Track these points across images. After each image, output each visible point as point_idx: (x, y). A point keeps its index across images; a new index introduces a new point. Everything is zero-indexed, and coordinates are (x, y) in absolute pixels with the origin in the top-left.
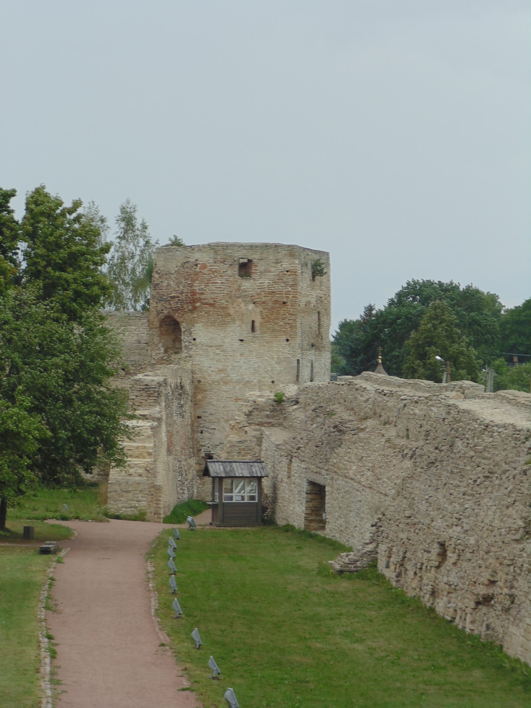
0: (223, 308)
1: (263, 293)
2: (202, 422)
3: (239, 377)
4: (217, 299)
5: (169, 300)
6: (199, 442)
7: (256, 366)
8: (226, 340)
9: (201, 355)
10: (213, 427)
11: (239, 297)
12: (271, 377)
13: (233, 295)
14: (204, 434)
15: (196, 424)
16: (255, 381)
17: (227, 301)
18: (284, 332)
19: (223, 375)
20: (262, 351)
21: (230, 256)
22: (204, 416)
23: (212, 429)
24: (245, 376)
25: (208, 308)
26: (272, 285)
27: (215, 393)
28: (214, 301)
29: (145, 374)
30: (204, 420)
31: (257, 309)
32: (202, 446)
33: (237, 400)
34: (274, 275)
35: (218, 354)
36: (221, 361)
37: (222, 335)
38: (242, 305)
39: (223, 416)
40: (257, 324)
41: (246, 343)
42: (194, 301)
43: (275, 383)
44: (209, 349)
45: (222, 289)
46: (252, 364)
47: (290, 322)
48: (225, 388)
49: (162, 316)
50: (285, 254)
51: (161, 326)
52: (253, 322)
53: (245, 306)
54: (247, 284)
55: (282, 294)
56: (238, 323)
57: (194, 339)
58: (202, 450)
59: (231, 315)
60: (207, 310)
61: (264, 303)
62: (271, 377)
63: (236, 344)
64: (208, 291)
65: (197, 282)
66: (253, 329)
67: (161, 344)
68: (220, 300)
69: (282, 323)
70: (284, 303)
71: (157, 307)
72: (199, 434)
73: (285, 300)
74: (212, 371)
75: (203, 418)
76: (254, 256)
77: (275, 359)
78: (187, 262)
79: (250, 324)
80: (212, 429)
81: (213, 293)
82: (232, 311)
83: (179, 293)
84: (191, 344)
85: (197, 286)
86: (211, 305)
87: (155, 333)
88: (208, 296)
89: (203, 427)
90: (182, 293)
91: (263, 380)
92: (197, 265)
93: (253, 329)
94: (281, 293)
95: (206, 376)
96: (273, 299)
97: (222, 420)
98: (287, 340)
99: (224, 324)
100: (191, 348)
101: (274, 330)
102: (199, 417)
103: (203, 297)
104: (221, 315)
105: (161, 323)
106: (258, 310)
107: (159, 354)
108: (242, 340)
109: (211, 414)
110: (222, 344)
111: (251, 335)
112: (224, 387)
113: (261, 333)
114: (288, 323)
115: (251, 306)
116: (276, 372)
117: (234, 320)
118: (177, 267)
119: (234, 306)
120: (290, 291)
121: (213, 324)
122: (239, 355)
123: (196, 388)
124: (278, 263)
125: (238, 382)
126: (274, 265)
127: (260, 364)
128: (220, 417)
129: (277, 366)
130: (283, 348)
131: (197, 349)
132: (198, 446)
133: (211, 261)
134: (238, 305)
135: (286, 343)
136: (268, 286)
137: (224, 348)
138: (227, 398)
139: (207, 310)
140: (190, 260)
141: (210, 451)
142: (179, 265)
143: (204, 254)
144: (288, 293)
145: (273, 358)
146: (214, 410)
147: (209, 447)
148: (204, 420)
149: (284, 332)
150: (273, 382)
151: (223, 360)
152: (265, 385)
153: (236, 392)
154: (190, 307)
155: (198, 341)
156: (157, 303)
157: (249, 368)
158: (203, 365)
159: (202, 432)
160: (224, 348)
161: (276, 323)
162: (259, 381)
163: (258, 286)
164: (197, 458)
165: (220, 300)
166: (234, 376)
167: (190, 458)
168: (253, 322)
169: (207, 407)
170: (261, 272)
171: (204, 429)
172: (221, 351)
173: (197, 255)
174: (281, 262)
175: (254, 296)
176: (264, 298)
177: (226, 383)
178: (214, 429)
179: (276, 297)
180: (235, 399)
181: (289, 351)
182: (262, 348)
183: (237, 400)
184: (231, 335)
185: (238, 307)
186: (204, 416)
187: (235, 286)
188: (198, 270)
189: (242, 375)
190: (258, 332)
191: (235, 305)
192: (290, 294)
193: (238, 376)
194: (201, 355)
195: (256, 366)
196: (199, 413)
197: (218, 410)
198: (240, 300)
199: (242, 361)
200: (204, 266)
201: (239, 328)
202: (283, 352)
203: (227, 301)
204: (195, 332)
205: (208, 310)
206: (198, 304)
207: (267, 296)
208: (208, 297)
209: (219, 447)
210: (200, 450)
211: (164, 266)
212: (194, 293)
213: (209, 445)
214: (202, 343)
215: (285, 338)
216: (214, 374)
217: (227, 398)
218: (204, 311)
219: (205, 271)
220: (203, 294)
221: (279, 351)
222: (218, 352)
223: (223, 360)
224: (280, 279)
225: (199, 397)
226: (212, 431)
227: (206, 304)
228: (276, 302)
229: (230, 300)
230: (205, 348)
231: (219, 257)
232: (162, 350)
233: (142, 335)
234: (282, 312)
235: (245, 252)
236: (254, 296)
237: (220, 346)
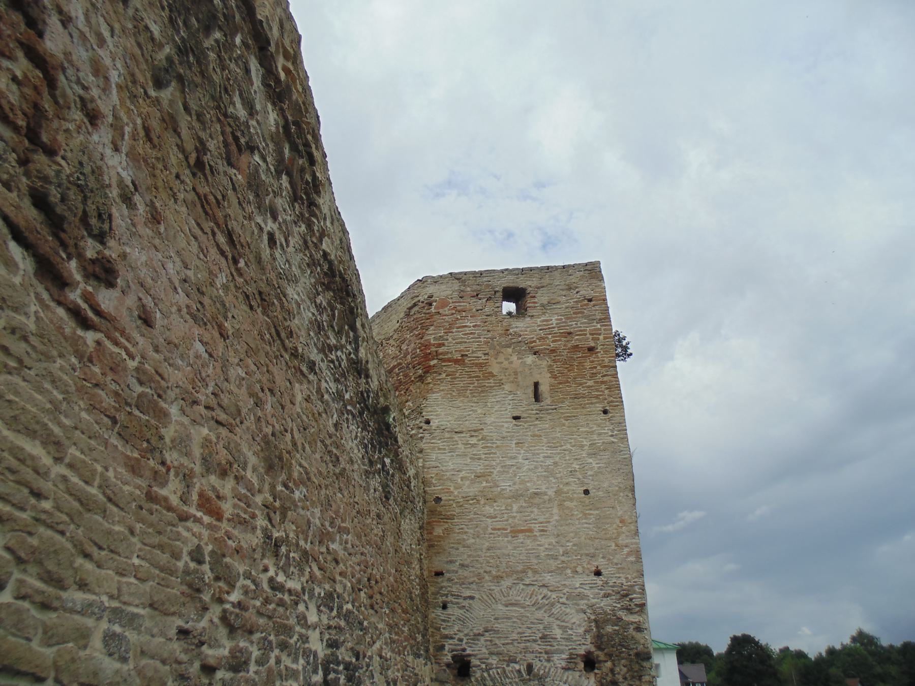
0: (480, 365)
2: (445, 584)
3: (516, 487)
6: (438, 629)
7: (549, 462)
8: (489, 420)
9: (439, 449)
10: (468, 593)
11: (508, 346)
12: (583, 483)
13: (495, 343)
14: (449, 611)
15: (432, 589)
16: (551, 492)
17: (485, 354)
18: (597, 397)
19: (484, 484)
20: (558, 435)
21: (488, 286)
22: (448, 571)
23: (465, 598)
24: (528, 484)
27: (471, 520)
28: (462, 356)
29: (216, 230)
30: (449, 580)
31: (540, 362)
32: (447, 637)
33: (515, 533)
35: (473, 446)
36: (479, 459)
38: (514, 358)
39: (488, 569)
40: (544, 388)
41: (526, 422)
42: (427, 357)
43: (591, 494)
44: (456, 437)
46: (542, 459)
47: (605, 379)
48: (489, 510)
50: (582, 276)
52: (536, 385)
53: (518, 359)
54: (520, 325)
55: (585, 335)
56: (507, 387)
57: (428, 422)
58: (447, 648)
59: (494, 376)
61: (553, 351)
62: (583, 483)
63: (506, 425)
64: (450, 339)
65: (432, 328)
66: (537, 397)
68: (473, 352)
69: (590, 383)
70: (591, 349)
72: (439, 611)
73: (593, 345)
74: (462, 479)
75: (447, 575)
76: (529, 283)
77: (586, 448)
78: (415, 305)
79: (532, 388)
80: (465, 598)
81: (461, 343)
82: (495, 369)
84: (421, 431)
85: (431, 336)
86: (456, 361)
88: (453, 349)
89: (447, 595)
91: (566, 489)
92: (430, 304)
93: (537, 397)
94: (582, 333)
95: (452, 489)
97: (487, 578)
98: (605, 412)
99: (482, 392)
100: (422, 438)
101: (576, 397)
102: (439, 574)
103: (441, 350)
104: (478, 377)
108: (516, 418)
109: (462, 565)
110: (482, 427)
111: (537, 406)
112: (487, 508)
113: (553, 401)
114: (602, 382)
115: (530, 359)
116: (590, 473)
117: (501, 384)
119: (499, 360)
120: (600, 329)
121: (461, 393)
122: (514, 446)
123: (432, 512)
124: (570, 289)
125: (516, 496)
126: (564, 293)
127: (557, 459)
128: (482, 571)
129: (591, 460)
130: (599, 425)
131: (433, 438)
132: (438, 638)
133: (456, 294)
134: (507, 359)
135: (602, 416)
137: (485, 433)
138: (494, 529)
140: (420, 298)
141: (464, 650)
142: (402, 315)
143: (443, 287)
144: (595, 334)
145: (583, 446)
146: (469, 556)
147: (461, 640)
148: (449, 580)
149: (597, 397)
150: (586, 492)
151: (483, 456)
152: (571, 500)
153: (515, 517)
157: (536, 468)
158: (444, 468)
159: (445, 607)
160: (485, 433)
161: (581, 384)
162: (558, 492)
163: (539, 326)
164: (436, 667)
165: (473, 352)
166: (506, 485)
167: (417, 656)
168: (536, 385)
169: (453, 552)
170: (542, 305)
171: (450, 598)
172: (479, 440)
173: (431, 289)
174: (577, 288)
175: (535, 342)
177: (492, 500)
178: (472, 598)
180: (511, 532)
181: (612, 431)
182: (558, 429)
183: (515, 533)
184: (497, 411)
185: (506, 363)
186: (448, 571)
187: (500, 329)
188: (433, 310)
189: (523, 482)
190: (547, 401)
191: (501, 358)
192: (600, 334)
193: (514, 484)
194: (439, 449)
195: (549, 462)
196: (438, 563)
197: (479, 556)
198: (510, 350)
199: (520, 457)
200: (444, 303)
201: (510, 397)
202: (600, 434)
203: (485, 354)
204: (430, 409)
206: (432, 363)
207: (560, 340)
208: (452, 347)
209: (482, 639)
210: (442, 647)
211: (379, 334)
212: (427, 346)
213: (461, 635)
215: (600, 407)
216: (467, 483)
217: (494, 529)
218: (445, 371)
219: (446, 310)
220: (444, 345)
221: (592, 433)
222: (474, 441)
223: (483, 456)
224: (579, 313)
225: (438, 531)
226: (466, 603)
227: (449, 360)
228: (576, 348)
229: (491, 352)
230: (447, 435)
231: (469, 289)
234: (588, 365)
235: (511, 277)
236: (535, 342)
237: (475, 431)
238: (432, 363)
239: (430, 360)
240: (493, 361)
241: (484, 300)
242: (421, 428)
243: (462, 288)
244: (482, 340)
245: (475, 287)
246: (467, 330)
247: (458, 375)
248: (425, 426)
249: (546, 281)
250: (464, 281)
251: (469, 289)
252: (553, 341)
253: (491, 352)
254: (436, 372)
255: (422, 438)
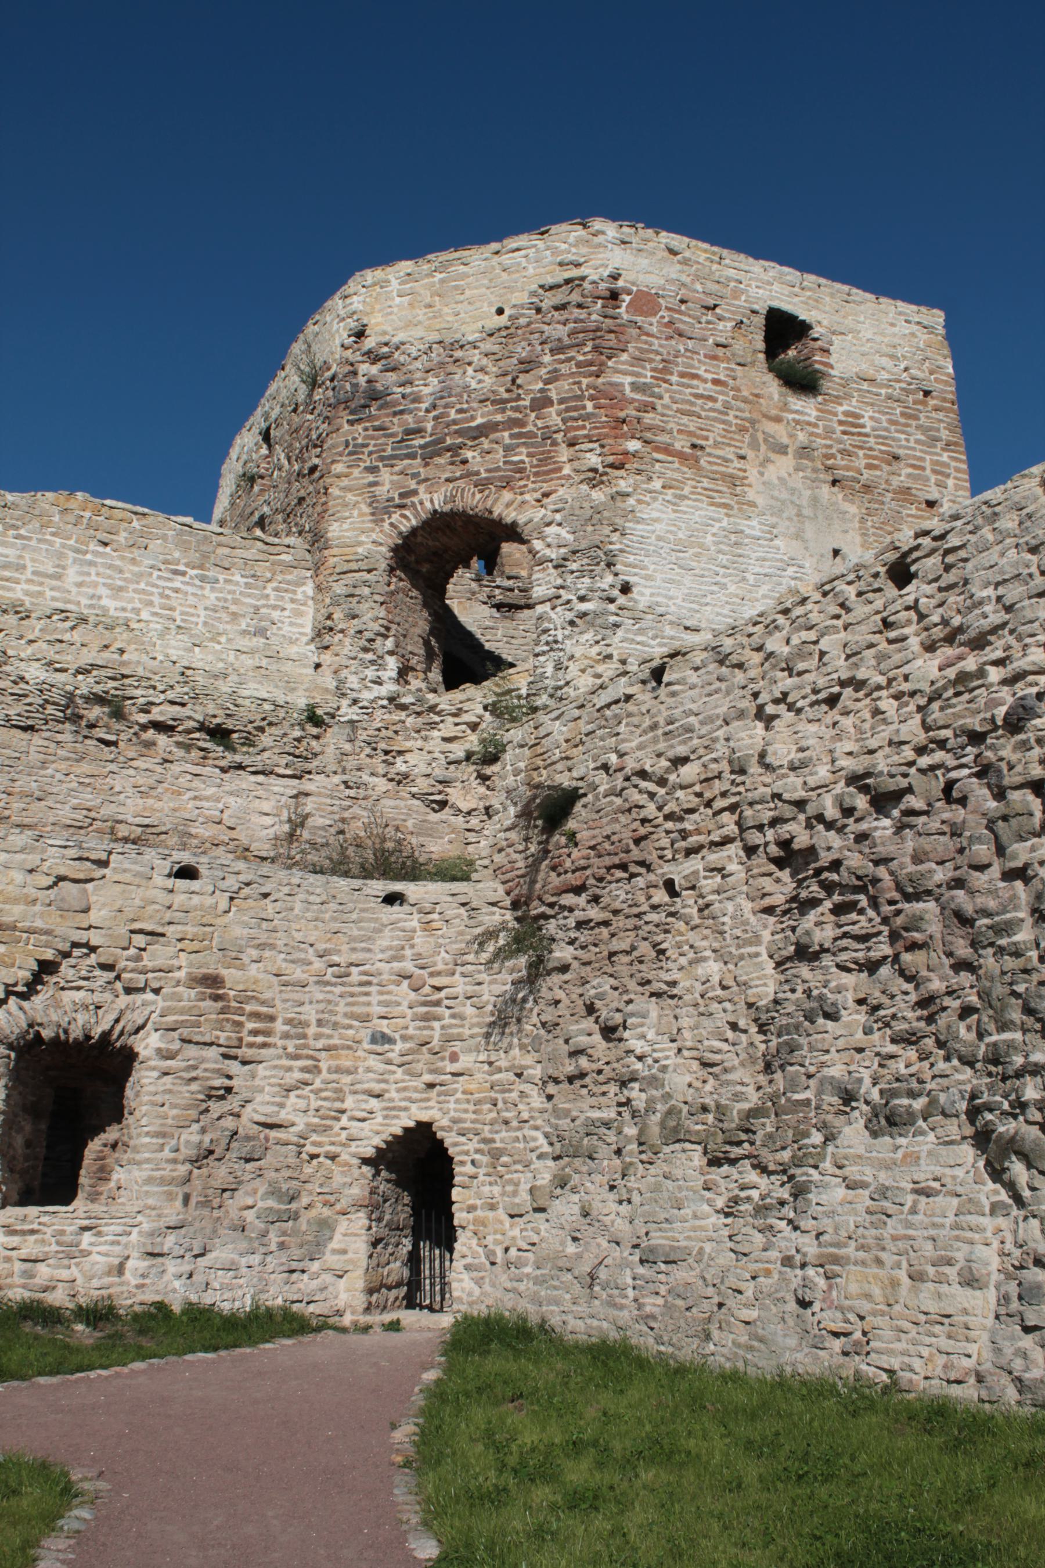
1: (861, 453)
4: (707, 439)
5: (454, 449)
25: (674, 470)
26: (886, 430)
28: (694, 446)
34: (889, 397)
37: (732, 589)
45: (719, 405)
49: (408, 521)
51: (392, 570)
57: (626, 589)
60: (670, 474)
61: (867, 488)
64: (666, 400)
65: (625, 357)
67: (390, 643)
68: (716, 445)
71: (375, 484)
73: (934, 494)
83: (517, 409)
84: (612, 607)
86: (682, 456)
87: (366, 591)
90: (541, 403)
92: (614, 296)
96: (896, 482)
100: (617, 625)
105: (396, 550)
106: (853, 509)
107: (378, 682)
118: (500, 311)
131: (641, 631)
136: (874, 429)
139: (670, 474)
142: (522, 297)
143: (644, 262)
154: (594, 460)
155: (642, 596)
156: (373, 470)
163: (841, 423)
176: (867, 474)
179: (903, 476)
200: (646, 302)
205: (676, 475)
206: (633, 445)
214: (660, 610)
219: (653, 324)
227: (667, 450)
228: (904, 493)
229: (750, 454)
232: (392, 664)
233: (276, 615)
236: (832, 456)
238: (633, 445)
239: (623, 436)
240: (753, 474)
241: (730, 325)
242: (612, 601)
243: (684, 278)
244: (730, 418)
245: (713, 287)
246: (702, 388)
247: (687, 490)
248: (622, 600)
249: (849, 322)
250: (686, 262)
251: (699, 287)
252: (869, 467)
253: (750, 454)
254: (639, 472)
255: (617, 625)
